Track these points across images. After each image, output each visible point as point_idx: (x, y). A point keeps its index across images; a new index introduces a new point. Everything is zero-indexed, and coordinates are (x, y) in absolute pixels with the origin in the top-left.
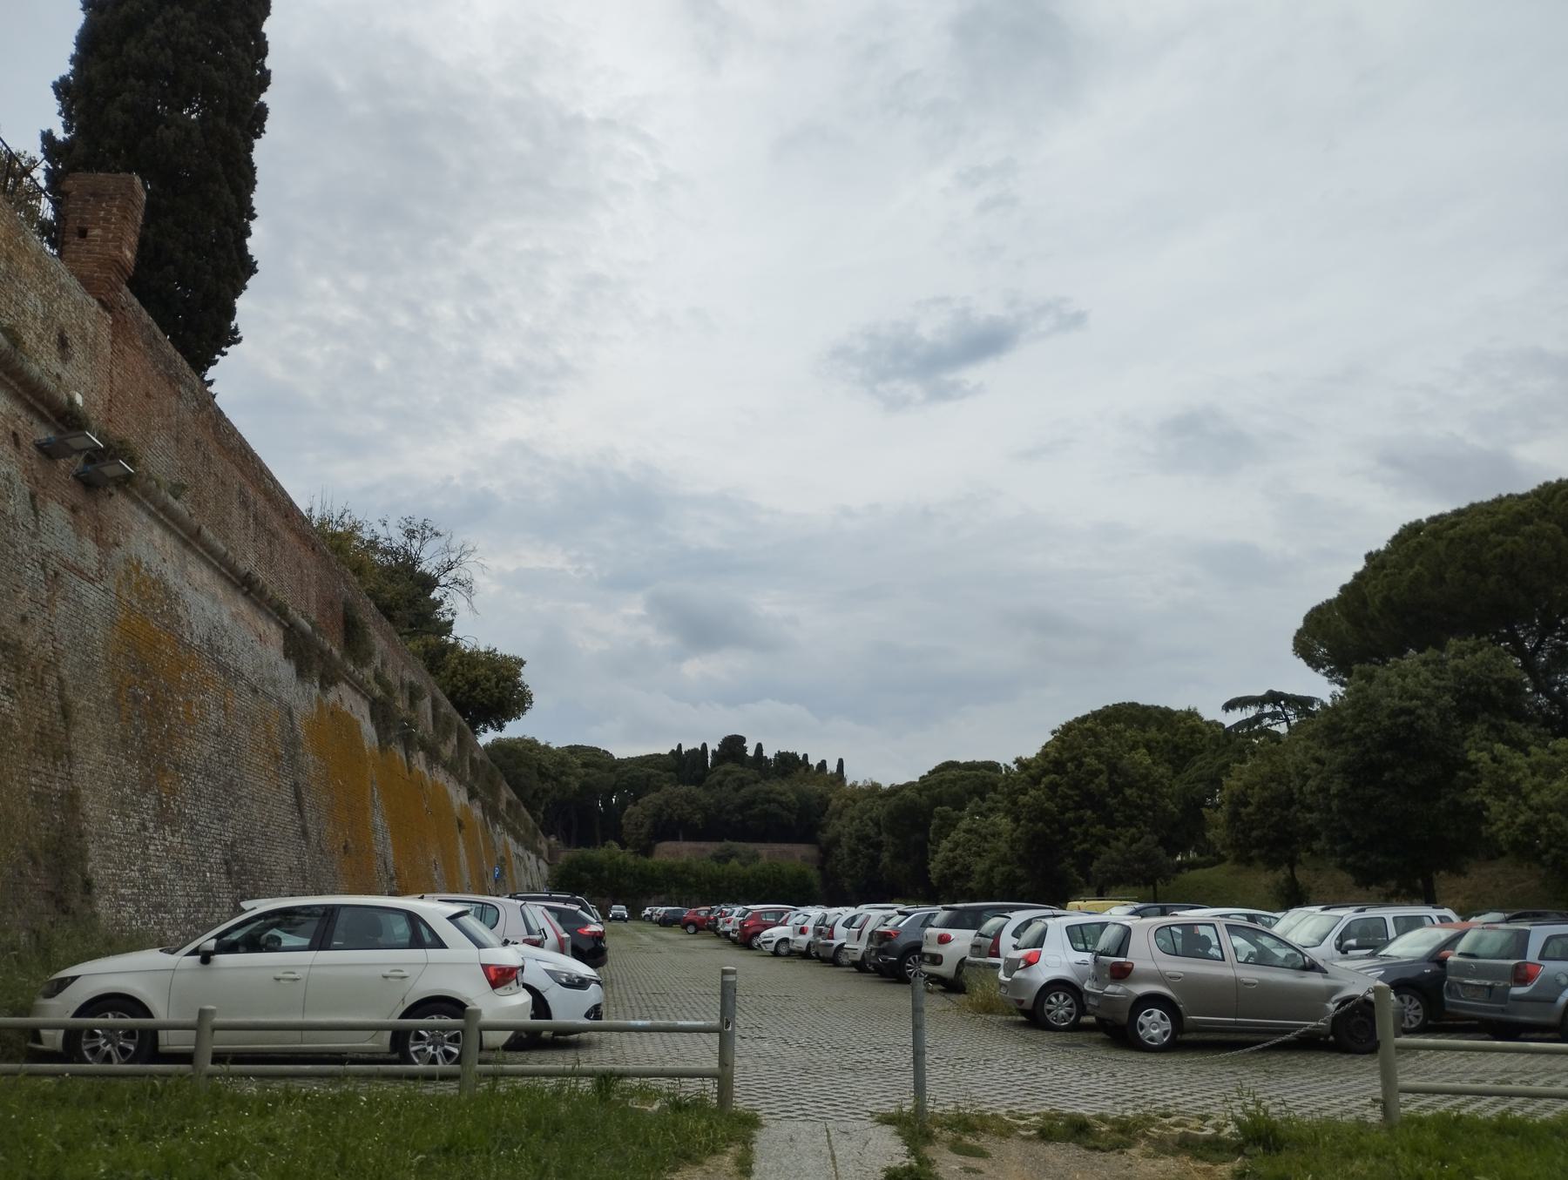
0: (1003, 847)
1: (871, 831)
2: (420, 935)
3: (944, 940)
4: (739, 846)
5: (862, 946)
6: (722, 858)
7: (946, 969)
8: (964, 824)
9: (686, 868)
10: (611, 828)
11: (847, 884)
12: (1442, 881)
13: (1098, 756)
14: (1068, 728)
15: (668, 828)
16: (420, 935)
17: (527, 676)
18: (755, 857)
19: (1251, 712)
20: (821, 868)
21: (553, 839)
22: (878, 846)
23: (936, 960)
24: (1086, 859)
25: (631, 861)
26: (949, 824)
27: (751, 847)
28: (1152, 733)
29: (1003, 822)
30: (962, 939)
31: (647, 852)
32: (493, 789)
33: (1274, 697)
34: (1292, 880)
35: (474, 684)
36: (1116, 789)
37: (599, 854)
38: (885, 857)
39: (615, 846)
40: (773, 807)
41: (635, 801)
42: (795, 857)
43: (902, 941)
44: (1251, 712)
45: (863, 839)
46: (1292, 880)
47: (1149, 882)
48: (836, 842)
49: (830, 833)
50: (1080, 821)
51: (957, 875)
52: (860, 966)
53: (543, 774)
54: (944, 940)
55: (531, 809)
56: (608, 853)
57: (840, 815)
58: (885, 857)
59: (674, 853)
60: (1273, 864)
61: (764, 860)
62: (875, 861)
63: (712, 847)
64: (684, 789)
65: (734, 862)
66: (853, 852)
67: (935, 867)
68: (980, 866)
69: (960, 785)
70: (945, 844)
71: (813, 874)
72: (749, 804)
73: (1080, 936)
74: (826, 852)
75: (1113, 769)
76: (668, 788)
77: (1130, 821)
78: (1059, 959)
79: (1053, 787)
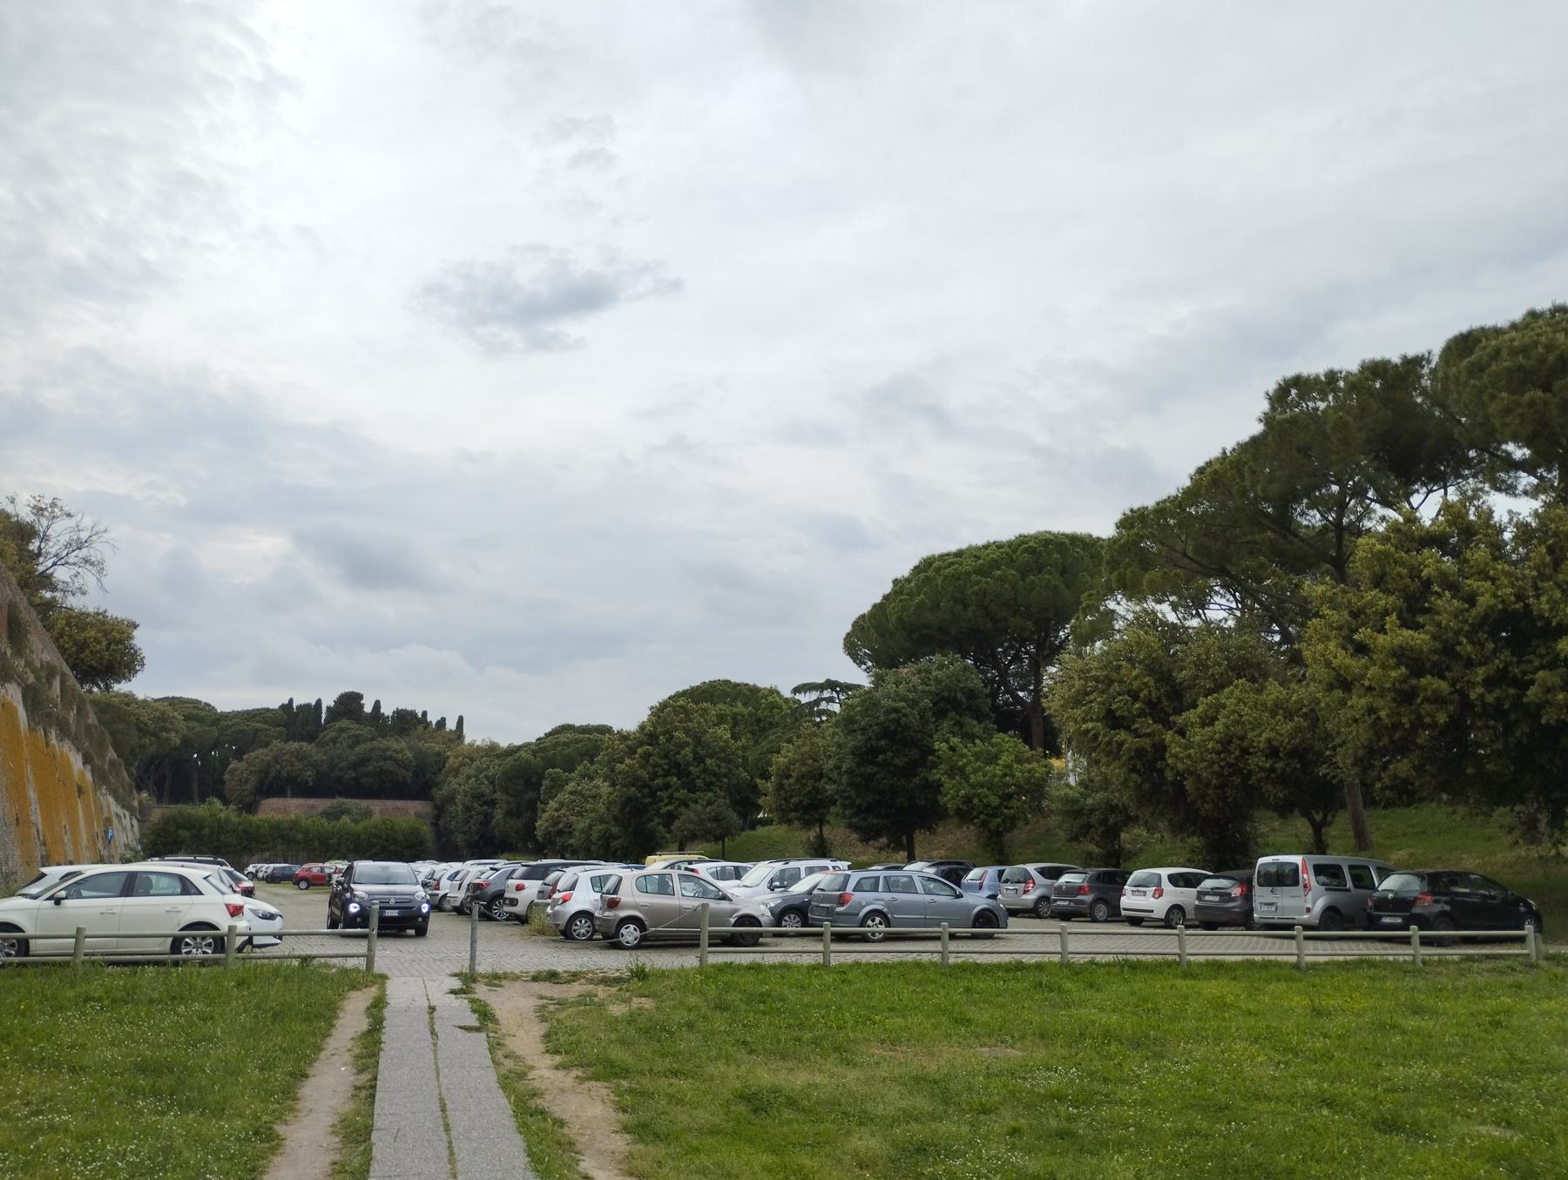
0: (601, 808)
1: (486, 788)
2: (187, 888)
3: (520, 888)
4: (350, 803)
5: (461, 895)
6: (333, 815)
7: (520, 909)
8: (571, 786)
9: (295, 825)
10: (213, 786)
11: (460, 839)
12: (919, 836)
13: (687, 731)
14: (664, 706)
15: (273, 786)
16: (187, 888)
17: (140, 639)
18: (368, 814)
19: (813, 696)
20: (435, 824)
21: (144, 795)
22: (493, 803)
23: (514, 902)
24: (670, 818)
25: (235, 819)
26: (558, 785)
27: (364, 803)
28: (740, 708)
29: (605, 788)
30: (533, 887)
31: (251, 808)
32: (101, 746)
33: (831, 685)
34: (820, 837)
35: (83, 646)
36: (699, 760)
37: (199, 810)
38: (498, 814)
39: (218, 804)
40: (388, 765)
41: (239, 755)
42: (409, 813)
43: (491, 890)
44: (813, 696)
45: (478, 796)
46: (820, 837)
47: (719, 838)
48: (451, 799)
49: (444, 791)
50: (667, 786)
51: (560, 833)
52: (460, 911)
53: (142, 730)
54: (520, 888)
55: (128, 765)
56: (212, 810)
57: (456, 772)
58: (498, 814)
59: (274, 810)
60: (807, 825)
61: (376, 818)
62: (488, 818)
63: (323, 804)
64: (294, 745)
65: (345, 819)
66: (468, 809)
67: (541, 824)
68: (581, 824)
69: (574, 748)
70: (553, 804)
71: (426, 829)
72: (363, 761)
73: (598, 882)
74: (440, 810)
75: (698, 742)
76: (277, 744)
77: (709, 786)
78: (585, 898)
79: (647, 756)
